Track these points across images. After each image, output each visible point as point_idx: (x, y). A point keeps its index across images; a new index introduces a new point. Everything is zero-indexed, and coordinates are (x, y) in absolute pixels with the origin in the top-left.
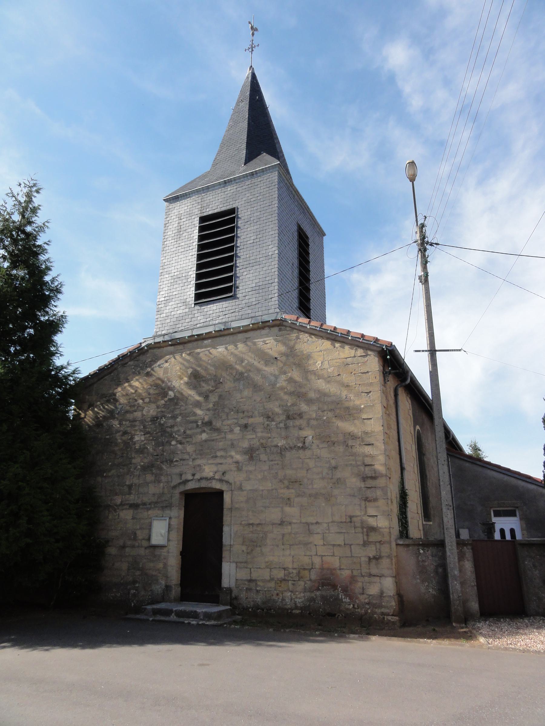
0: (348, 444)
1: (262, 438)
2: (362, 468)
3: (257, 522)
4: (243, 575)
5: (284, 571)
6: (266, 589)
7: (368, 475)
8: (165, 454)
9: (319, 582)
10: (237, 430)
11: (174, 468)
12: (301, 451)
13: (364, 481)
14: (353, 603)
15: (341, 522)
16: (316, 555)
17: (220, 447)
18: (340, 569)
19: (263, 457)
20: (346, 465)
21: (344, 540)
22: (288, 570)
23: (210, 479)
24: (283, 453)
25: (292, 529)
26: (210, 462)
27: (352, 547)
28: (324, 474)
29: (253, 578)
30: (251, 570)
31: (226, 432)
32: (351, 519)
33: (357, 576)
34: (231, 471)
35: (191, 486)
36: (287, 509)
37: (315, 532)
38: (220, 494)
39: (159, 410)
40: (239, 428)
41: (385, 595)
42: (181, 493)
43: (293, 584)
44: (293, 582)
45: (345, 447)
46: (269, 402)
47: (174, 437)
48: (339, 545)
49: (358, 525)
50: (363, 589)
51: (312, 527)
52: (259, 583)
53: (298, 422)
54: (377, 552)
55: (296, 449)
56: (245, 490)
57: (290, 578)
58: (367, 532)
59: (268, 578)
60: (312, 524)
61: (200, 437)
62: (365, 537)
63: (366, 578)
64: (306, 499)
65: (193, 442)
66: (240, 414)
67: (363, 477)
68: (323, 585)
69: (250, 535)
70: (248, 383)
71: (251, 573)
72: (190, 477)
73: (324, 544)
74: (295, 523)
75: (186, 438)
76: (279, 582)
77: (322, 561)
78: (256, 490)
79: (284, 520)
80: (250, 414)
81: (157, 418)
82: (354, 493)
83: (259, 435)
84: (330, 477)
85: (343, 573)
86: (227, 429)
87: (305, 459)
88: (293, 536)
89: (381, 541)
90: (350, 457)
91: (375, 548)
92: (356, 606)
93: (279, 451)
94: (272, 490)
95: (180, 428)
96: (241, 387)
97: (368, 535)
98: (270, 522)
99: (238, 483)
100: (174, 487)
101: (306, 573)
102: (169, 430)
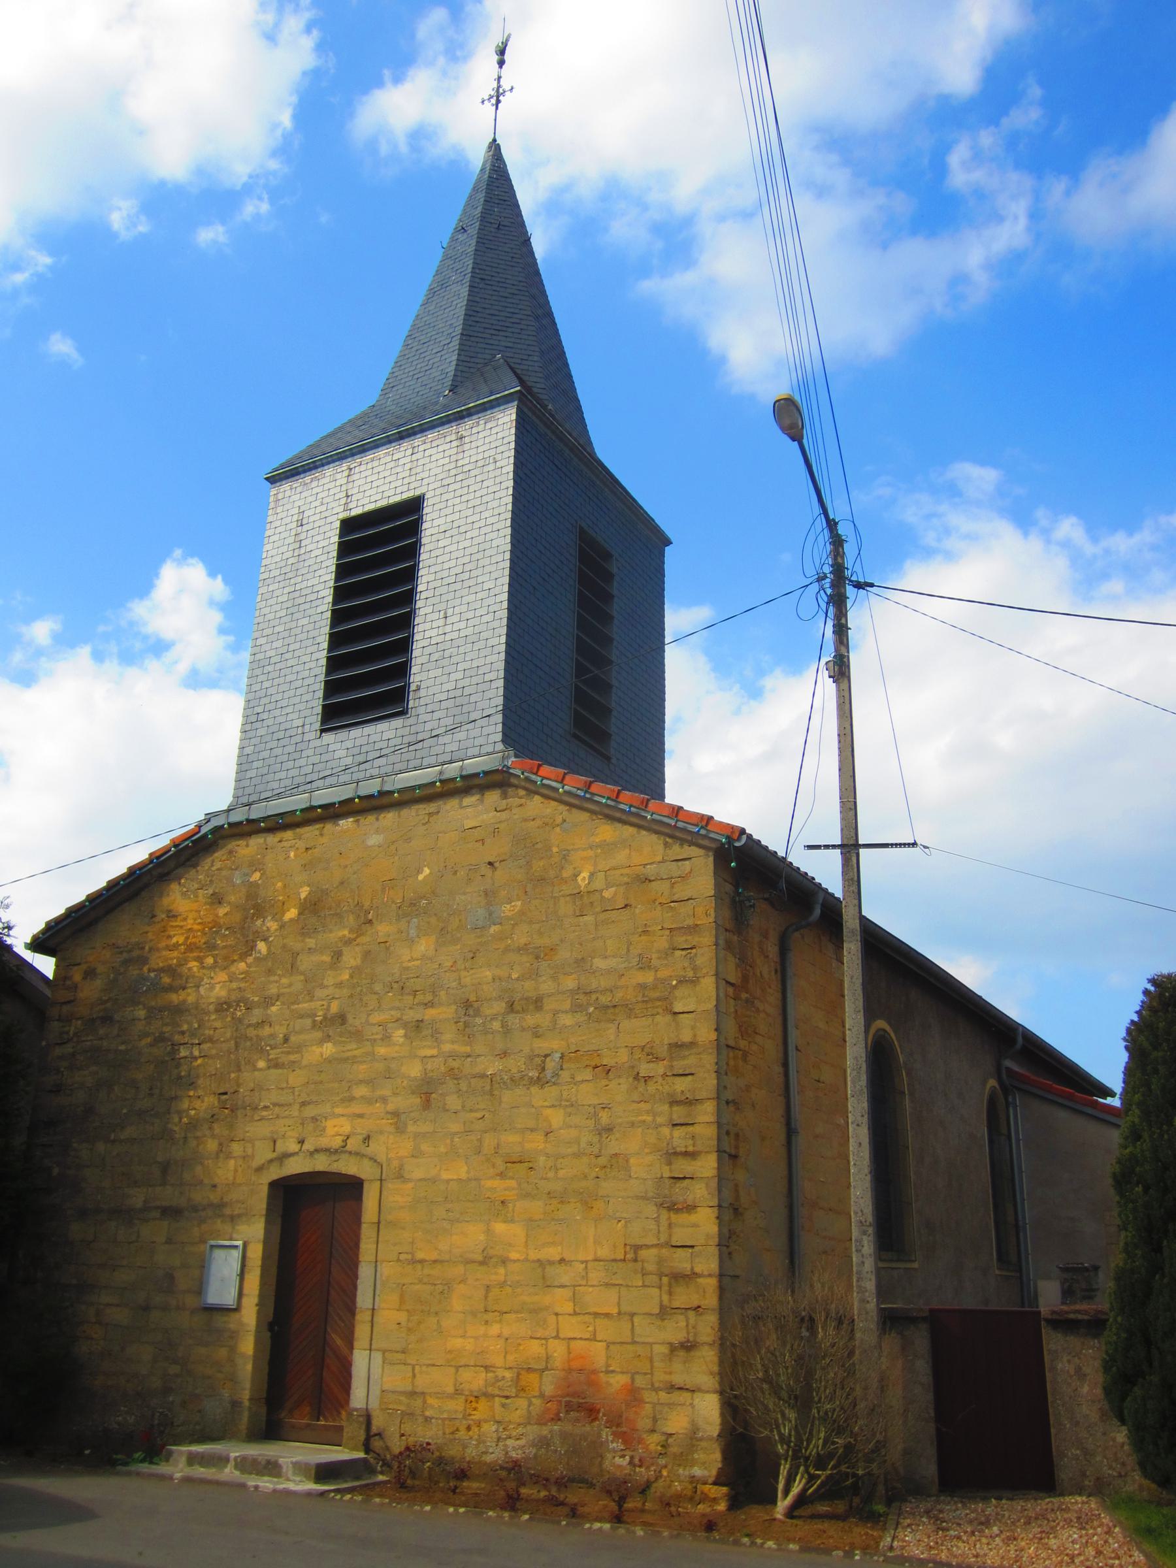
0: (638, 1073)
1: (453, 1055)
2: (666, 1131)
3: (434, 1256)
4: (396, 1379)
5: (486, 1372)
6: (445, 1416)
7: (678, 1150)
8: (241, 1090)
9: (560, 1401)
10: (399, 1034)
11: (259, 1123)
12: (534, 1089)
13: (669, 1163)
14: (631, 1453)
15: (615, 1260)
16: (557, 1337)
17: (361, 1077)
18: (608, 1372)
19: (453, 1102)
20: (633, 1124)
21: (619, 1304)
22: (494, 1372)
23: (336, 1151)
24: (496, 1092)
25: (506, 1275)
26: (338, 1110)
27: (636, 1319)
28: (583, 1145)
29: (419, 1390)
30: (413, 1370)
31: (375, 1040)
32: (635, 1253)
33: (643, 1389)
34: (381, 1132)
35: (296, 1166)
36: (500, 1227)
37: (556, 1283)
38: (352, 1188)
39: (234, 985)
40: (401, 1032)
41: (700, 1434)
42: (274, 1185)
43: (503, 1405)
44: (504, 1400)
45: (631, 1079)
46: (472, 969)
47: (262, 1050)
48: (607, 1315)
49: (651, 1267)
50: (653, 1420)
51: (550, 1270)
52: (430, 1401)
53: (531, 1020)
54: (688, 1333)
55: (524, 1082)
56: (410, 1180)
57: (497, 1392)
58: (670, 1285)
59: (450, 1389)
60: (551, 1263)
61: (317, 1050)
62: (665, 1298)
63: (663, 1395)
64: (540, 1203)
65: (304, 1062)
66: (405, 997)
67: (667, 1153)
68: (569, 1407)
69: (417, 1287)
70: (428, 923)
71: (414, 1376)
72: (293, 1147)
73: (574, 1310)
74: (515, 1261)
75: (289, 1053)
76: (473, 1399)
77: (570, 1353)
78: (434, 1181)
79: (491, 1252)
80: (429, 997)
81: (229, 1005)
82: (646, 1192)
83: (447, 1047)
84: (596, 1150)
85: (612, 1381)
86: (377, 1034)
87: (542, 1107)
88: (509, 1290)
89: (699, 1307)
90: (642, 1105)
91: (684, 1324)
92: (636, 1461)
93: (488, 1088)
94: (469, 1180)
95: (277, 1028)
96: (413, 932)
97: (670, 1293)
98: (461, 1256)
99: (395, 1163)
100: (259, 1169)
101: (533, 1378)
102: (251, 1032)
